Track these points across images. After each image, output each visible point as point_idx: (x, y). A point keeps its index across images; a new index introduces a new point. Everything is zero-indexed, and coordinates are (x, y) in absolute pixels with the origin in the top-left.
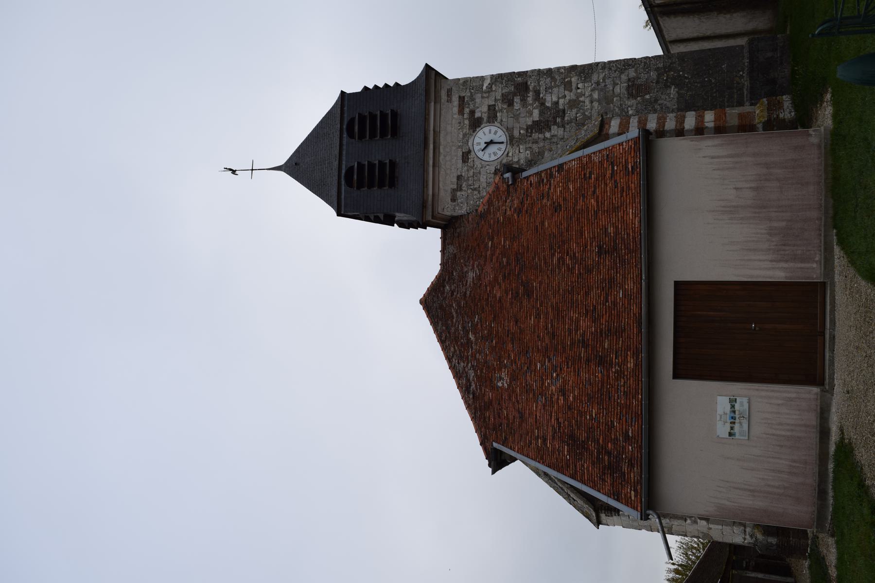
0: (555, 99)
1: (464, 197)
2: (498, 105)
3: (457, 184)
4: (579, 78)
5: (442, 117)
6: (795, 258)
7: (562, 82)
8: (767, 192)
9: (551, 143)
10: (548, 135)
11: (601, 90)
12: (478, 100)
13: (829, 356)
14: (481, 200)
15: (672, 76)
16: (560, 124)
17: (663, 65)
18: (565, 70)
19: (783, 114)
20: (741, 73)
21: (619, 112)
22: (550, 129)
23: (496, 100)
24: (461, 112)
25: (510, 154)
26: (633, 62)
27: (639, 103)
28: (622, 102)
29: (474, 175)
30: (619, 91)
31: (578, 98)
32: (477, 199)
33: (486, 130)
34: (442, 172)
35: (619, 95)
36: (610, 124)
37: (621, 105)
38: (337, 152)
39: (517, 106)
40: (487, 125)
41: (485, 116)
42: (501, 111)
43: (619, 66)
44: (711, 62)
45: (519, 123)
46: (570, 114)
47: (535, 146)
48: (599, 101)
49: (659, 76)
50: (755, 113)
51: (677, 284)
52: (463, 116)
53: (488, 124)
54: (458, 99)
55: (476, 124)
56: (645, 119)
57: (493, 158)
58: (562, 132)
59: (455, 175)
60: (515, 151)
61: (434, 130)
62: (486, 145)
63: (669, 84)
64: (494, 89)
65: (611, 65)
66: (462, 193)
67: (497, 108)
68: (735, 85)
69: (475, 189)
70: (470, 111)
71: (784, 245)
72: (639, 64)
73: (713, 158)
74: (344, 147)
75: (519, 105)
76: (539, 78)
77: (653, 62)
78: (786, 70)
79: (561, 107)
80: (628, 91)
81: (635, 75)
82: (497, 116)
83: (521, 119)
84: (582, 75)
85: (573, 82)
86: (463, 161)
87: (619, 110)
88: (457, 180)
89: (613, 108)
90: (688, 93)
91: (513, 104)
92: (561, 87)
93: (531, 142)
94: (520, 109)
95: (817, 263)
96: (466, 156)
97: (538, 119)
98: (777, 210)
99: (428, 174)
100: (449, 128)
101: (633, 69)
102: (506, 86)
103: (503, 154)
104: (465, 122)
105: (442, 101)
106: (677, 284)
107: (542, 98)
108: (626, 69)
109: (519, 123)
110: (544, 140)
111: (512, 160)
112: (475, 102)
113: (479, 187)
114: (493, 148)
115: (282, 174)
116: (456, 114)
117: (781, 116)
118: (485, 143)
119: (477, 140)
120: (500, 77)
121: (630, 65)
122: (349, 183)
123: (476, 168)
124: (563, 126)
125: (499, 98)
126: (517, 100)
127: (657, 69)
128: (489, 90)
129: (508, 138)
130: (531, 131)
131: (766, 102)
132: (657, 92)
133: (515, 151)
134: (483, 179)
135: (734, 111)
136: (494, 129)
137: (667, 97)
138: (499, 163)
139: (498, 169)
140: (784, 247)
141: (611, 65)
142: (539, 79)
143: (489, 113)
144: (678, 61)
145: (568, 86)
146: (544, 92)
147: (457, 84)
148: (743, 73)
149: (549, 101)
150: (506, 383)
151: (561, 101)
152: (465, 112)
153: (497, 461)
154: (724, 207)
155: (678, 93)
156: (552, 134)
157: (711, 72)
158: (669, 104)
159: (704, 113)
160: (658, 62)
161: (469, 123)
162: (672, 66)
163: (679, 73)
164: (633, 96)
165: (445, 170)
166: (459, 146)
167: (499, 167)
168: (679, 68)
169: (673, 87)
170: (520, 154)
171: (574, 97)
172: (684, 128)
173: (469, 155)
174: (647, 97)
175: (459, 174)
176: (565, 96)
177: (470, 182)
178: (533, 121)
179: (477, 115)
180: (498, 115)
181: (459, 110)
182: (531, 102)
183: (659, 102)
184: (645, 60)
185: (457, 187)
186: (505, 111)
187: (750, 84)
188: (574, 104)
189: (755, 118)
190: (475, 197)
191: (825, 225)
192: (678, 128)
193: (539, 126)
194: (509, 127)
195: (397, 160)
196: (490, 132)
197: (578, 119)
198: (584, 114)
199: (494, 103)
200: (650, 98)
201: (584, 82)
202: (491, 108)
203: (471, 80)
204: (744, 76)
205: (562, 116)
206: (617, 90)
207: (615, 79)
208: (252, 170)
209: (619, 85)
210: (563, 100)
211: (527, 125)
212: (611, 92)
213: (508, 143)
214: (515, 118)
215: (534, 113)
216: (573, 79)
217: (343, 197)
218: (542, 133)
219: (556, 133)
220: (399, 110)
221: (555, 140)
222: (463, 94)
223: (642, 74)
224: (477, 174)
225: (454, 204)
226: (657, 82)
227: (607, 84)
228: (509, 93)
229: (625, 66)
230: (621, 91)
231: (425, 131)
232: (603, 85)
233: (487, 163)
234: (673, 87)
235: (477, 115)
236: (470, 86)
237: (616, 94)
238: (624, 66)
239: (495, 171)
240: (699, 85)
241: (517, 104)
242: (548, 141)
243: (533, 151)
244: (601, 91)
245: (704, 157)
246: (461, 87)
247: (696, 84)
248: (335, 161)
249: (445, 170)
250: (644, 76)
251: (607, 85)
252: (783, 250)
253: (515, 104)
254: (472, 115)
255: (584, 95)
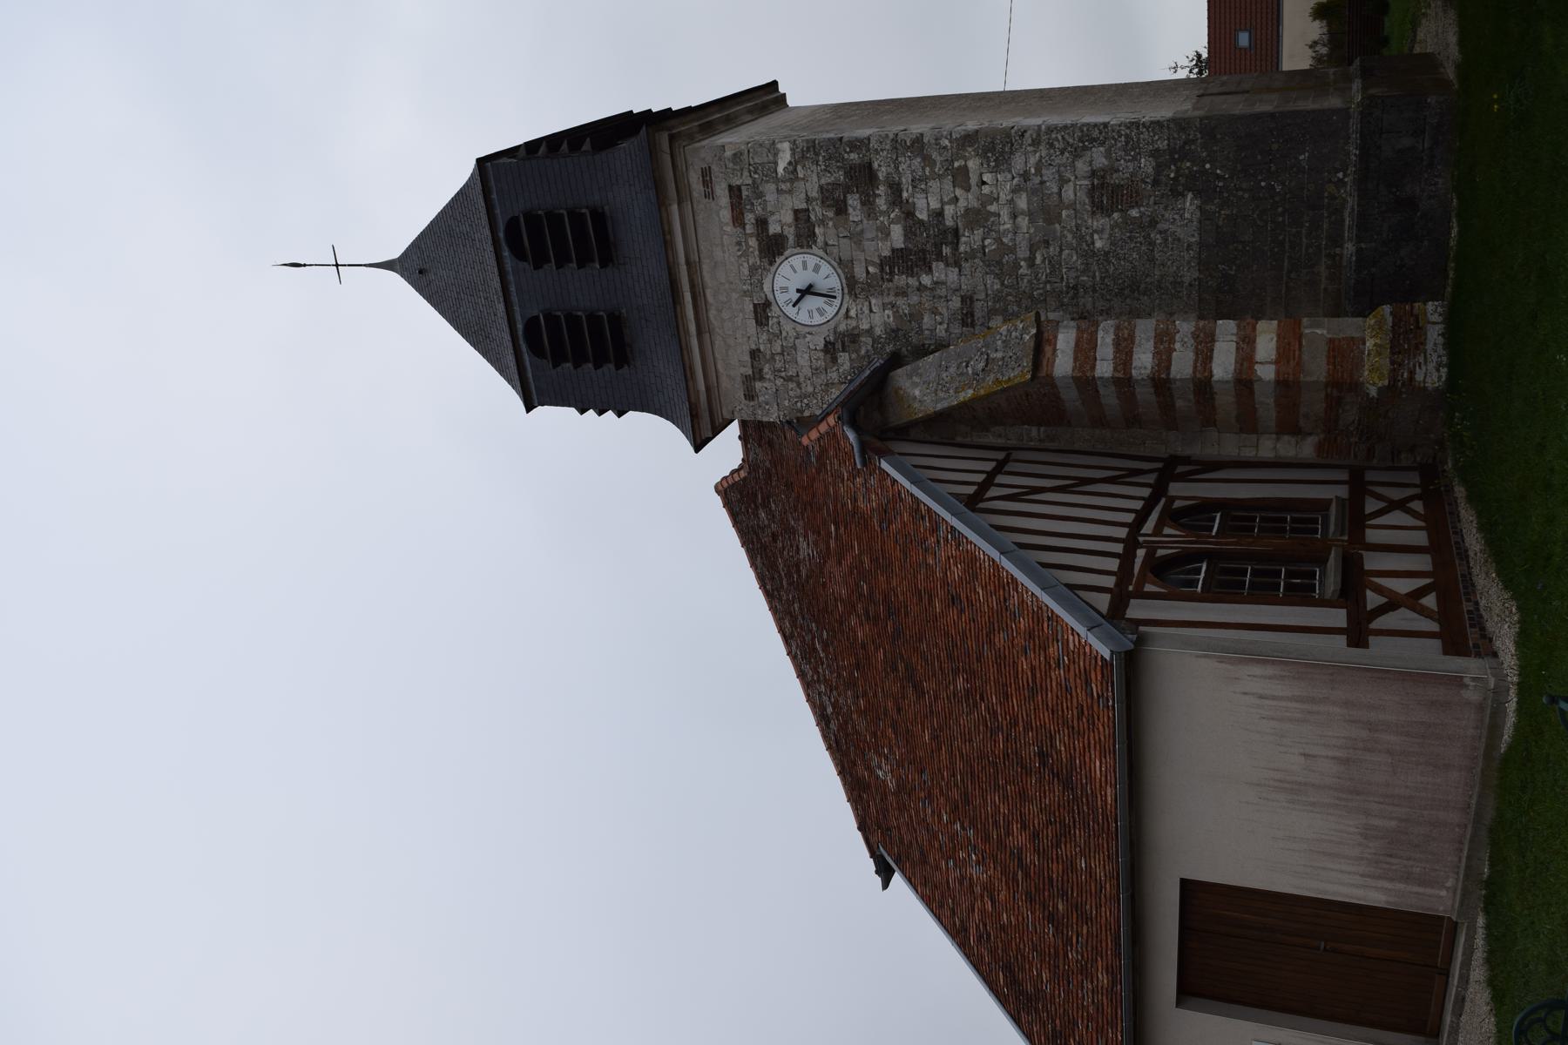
0: (935, 205)
1: (770, 392)
2: (814, 210)
3: (752, 366)
4: (984, 162)
5: (700, 231)
6: (1407, 878)
7: (947, 169)
8: (1367, 769)
9: (934, 297)
10: (926, 280)
11: (1034, 192)
12: (771, 197)
13: (1452, 1021)
14: (805, 401)
15: (1187, 171)
16: (951, 261)
17: (1168, 145)
18: (950, 142)
19: (1424, 368)
20: (1340, 175)
21: (1074, 241)
22: (930, 268)
23: (808, 200)
24: (738, 220)
25: (853, 313)
26: (1100, 133)
27: (1116, 225)
28: (1079, 222)
29: (783, 351)
30: (1072, 197)
31: (984, 205)
32: (797, 397)
33: (796, 261)
34: (718, 342)
35: (1072, 206)
36: (1055, 344)
37: (1077, 226)
38: (496, 283)
39: (855, 212)
40: (796, 251)
41: (790, 233)
42: (822, 222)
43: (1071, 141)
44: (1275, 146)
45: (864, 251)
46: (970, 240)
47: (900, 301)
48: (1031, 214)
49: (1159, 168)
50: (1364, 344)
51: (1185, 884)
52: (744, 229)
53: (798, 250)
54: (727, 191)
55: (773, 248)
56: (1129, 334)
57: (818, 320)
58: (956, 278)
59: (746, 348)
60: (861, 309)
61: (688, 263)
62: (799, 294)
63: (1180, 188)
64: (801, 175)
65: (1054, 136)
66: (765, 385)
67: (813, 217)
68: (1326, 200)
69: (789, 379)
70: (757, 220)
71: (1391, 856)
72: (1113, 138)
73: (1261, 697)
74: (511, 278)
75: (859, 213)
76: (897, 157)
77: (1147, 137)
78: (1440, 181)
79: (949, 223)
80: (1093, 197)
81: (1106, 163)
82: (814, 233)
83: (866, 244)
84: (990, 155)
85: (971, 171)
86: (757, 322)
87: (1073, 238)
88: (751, 358)
89: (1061, 232)
90: (1223, 212)
91: (846, 210)
92: (945, 181)
93: (892, 293)
94: (861, 221)
95: (1447, 891)
96: (762, 312)
97: (903, 246)
98: (1382, 800)
99: (690, 352)
100: (718, 253)
101: (1101, 149)
102: (825, 170)
103: (837, 313)
104: (750, 243)
105: (695, 194)
106: (1185, 884)
107: (907, 201)
108: (1085, 148)
109: (864, 251)
110: (918, 290)
111: (857, 327)
112: (765, 200)
113: (798, 376)
114: (812, 302)
115: (394, 279)
116: (727, 224)
117: (1419, 377)
118: (798, 291)
119: (780, 282)
120: (812, 149)
121: (1095, 140)
122: (536, 349)
123: (785, 337)
124: (957, 264)
125: (815, 194)
126: (853, 201)
127: (1155, 154)
128: (792, 176)
129: (844, 281)
130: (890, 269)
131: (1390, 319)
132: (1155, 204)
133: (861, 309)
134: (803, 360)
135: (1319, 332)
136: (812, 260)
137: (1176, 217)
138: (832, 331)
139: (830, 343)
140: (1389, 859)
141: (1054, 136)
142: (897, 159)
143: (796, 227)
144: (1202, 138)
145: (961, 177)
146: (910, 188)
147: (720, 159)
148: (1345, 176)
149: (923, 207)
150: (892, 783)
151: (949, 210)
152: (746, 221)
153: (885, 873)
154: (1281, 781)
155: (1201, 210)
156: (935, 279)
157: (1273, 168)
158: (1180, 233)
159: (1254, 329)
160: (1157, 137)
161: (760, 244)
162: (1187, 147)
163: (1204, 166)
164: (1102, 209)
165: (722, 337)
166: (745, 292)
167: (832, 339)
168: (1204, 154)
169: (1190, 196)
170: (872, 315)
171: (975, 204)
172: (1212, 376)
173: (768, 310)
174: (1134, 213)
175: (753, 347)
176: (956, 199)
177: (778, 365)
178: (893, 250)
179: (774, 228)
180: (817, 230)
181: (733, 217)
182: (884, 208)
183: (1159, 226)
184: (1128, 131)
185: (753, 372)
186: (831, 224)
187: (1358, 206)
188: (978, 217)
189: (1363, 359)
190: (791, 393)
191: (1472, 841)
192: (1198, 375)
193: (906, 261)
194: (842, 259)
195: (624, 311)
196: (805, 267)
197: (987, 250)
198: (998, 240)
199: (804, 206)
200: (1141, 217)
201: (995, 170)
202: (801, 215)
203: (749, 151)
204: (1346, 183)
205: (952, 243)
206: (1069, 193)
207: (1062, 169)
208: (337, 265)
209: (1071, 183)
210: (952, 207)
211: (879, 256)
212: (1056, 197)
213: (846, 291)
214: (855, 240)
215: (892, 233)
216: (971, 164)
217: (530, 375)
218: (912, 276)
219: (943, 277)
220: (606, 208)
221: (943, 292)
222: (736, 182)
223: (1122, 161)
224: (789, 351)
225: (752, 403)
226: (1156, 183)
227: (1045, 178)
228: (836, 185)
229: (1083, 142)
230: (1076, 195)
231: (669, 269)
232: (1037, 180)
233: (807, 330)
234: (1190, 196)
235: (774, 228)
236: (750, 165)
237: (1066, 201)
238: (1081, 140)
239: (825, 346)
240: (1246, 196)
241: (854, 210)
242: (928, 293)
243: (897, 311)
244: (1032, 193)
245: (1245, 694)
246: (731, 165)
247: (1240, 193)
248: (499, 302)
249: (722, 337)
250: (1126, 167)
251: (1045, 182)
252: (1387, 863)
253: (850, 210)
254: (762, 228)
255: (997, 199)
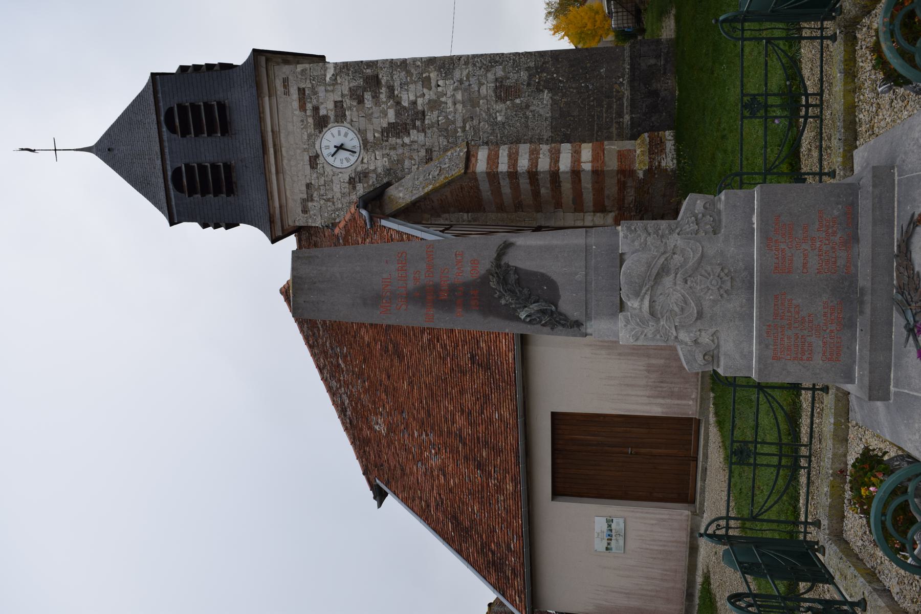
0: (412, 98)
2: (345, 101)
6: (672, 395)
7: (419, 78)
9: (411, 150)
10: (407, 140)
11: (465, 90)
12: (322, 94)
13: (701, 485)
14: (337, 213)
15: (544, 78)
16: (420, 129)
17: (535, 64)
18: (421, 63)
19: (665, 160)
20: (621, 80)
21: (486, 117)
22: (409, 133)
23: (343, 95)
24: (303, 107)
25: (365, 161)
26: (500, 58)
29: (325, 183)
30: (485, 93)
32: (332, 211)
33: (335, 131)
34: (288, 179)
35: (485, 97)
36: (477, 157)
37: (488, 109)
38: (157, 148)
40: (334, 125)
41: (332, 115)
42: (350, 108)
43: (485, 62)
45: (372, 124)
46: (431, 117)
47: (392, 153)
49: (530, 77)
50: (636, 152)
51: (554, 415)
52: (306, 112)
53: (336, 124)
55: (321, 123)
57: (346, 164)
59: (304, 183)
61: (273, 131)
62: (336, 149)
63: (541, 87)
64: (339, 82)
65: (476, 60)
66: (314, 204)
67: (345, 105)
68: (615, 93)
69: (328, 200)
70: (313, 107)
71: (662, 382)
72: (507, 61)
74: (166, 144)
78: (669, 81)
79: (420, 108)
81: (503, 74)
82: (345, 115)
83: (374, 120)
84: (442, 70)
87: (486, 115)
91: (364, 101)
93: (388, 148)
94: (372, 107)
95: (693, 400)
96: (314, 161)
97: (394, 121)
104: (309, 121)
105: (279, 93)
106: (554, 415)
107: (397, 96)
108: (492, 66)
109: (372, 124)
110: (402, 146)
111: (368, 168)
113: (333, 198)
114: (342, 154)
116: (296, 110)
117: (663, 164)
118: (335, 147)
119: (325, 143)
121: (497, 62)
122: (178, 186)
123: (327, 176)
124: (424, 131)
126: (368, 96)
127: (528, 69)
128: (334, 82)
129: (361, 142)
131: (648, 139)
134: (336, 188)
135: (613, 147)
136: (343, 130)
137: (539, 103)
138: (353, 171)
139: (352, 178)
140: (662, 385)
141: (476, 60)
143: (336, 111)
145: (426, 82)
146: (399, 88)
147: (294, 73)
148: (623, 80)
150: (384, 430)
151: (420, 101)
152: (307, 108)
153: (380, 496)
157: (588, 77)
158: (542, 112)
159: (580, 147)
162: (544, 66)
166: (305, 149)
167: (353, 175)
168: (553, 69)
169: (546, 91)
171: (434, 97)
174: (518, 101)
175: (308, 182)
177: (322, 192)
178: (389, 124)
179: (323, 112)
180: (347, 113)
182: (384, 100)
183: (531, 108)
186: (355, 109)
188: (435, 104)
189: (635, 159)
190: (329, 209)
192: (552, 169)
193: (396, 129)
195: (233, 162)
196: (339, 134)
198: (446, 117)
199: (340, 99)
201: (445, 79)
202: (338, 104)
207: (480, 77)
209: (485, 86)
210: (422, 99)
211: (381, 127)
212: (477, 93)
213: (362, 147)
215: (389, 114)
216: (432, 75)
217: (173, 203)
218: (399, 138)
219: (416, 138)
220: (226, 101)
221: (415, 146)
222: (302, 86)
224: (328, 183)
225: (306, 216)
226: (529, 85)
227: (471, 83)
228: (358, 87)
229: (491, 63)
231: (262, 133)
232: (467, 83)
233: (340, 170)
234: (546, 91)
235: (323, 112)
238: (490, 62)
239: (350, 179)
240: (575, 91)
246: (300, 76)
247: (572, 90)
250: (513, 77)
252: (661, 387)
253: (366, 101)
